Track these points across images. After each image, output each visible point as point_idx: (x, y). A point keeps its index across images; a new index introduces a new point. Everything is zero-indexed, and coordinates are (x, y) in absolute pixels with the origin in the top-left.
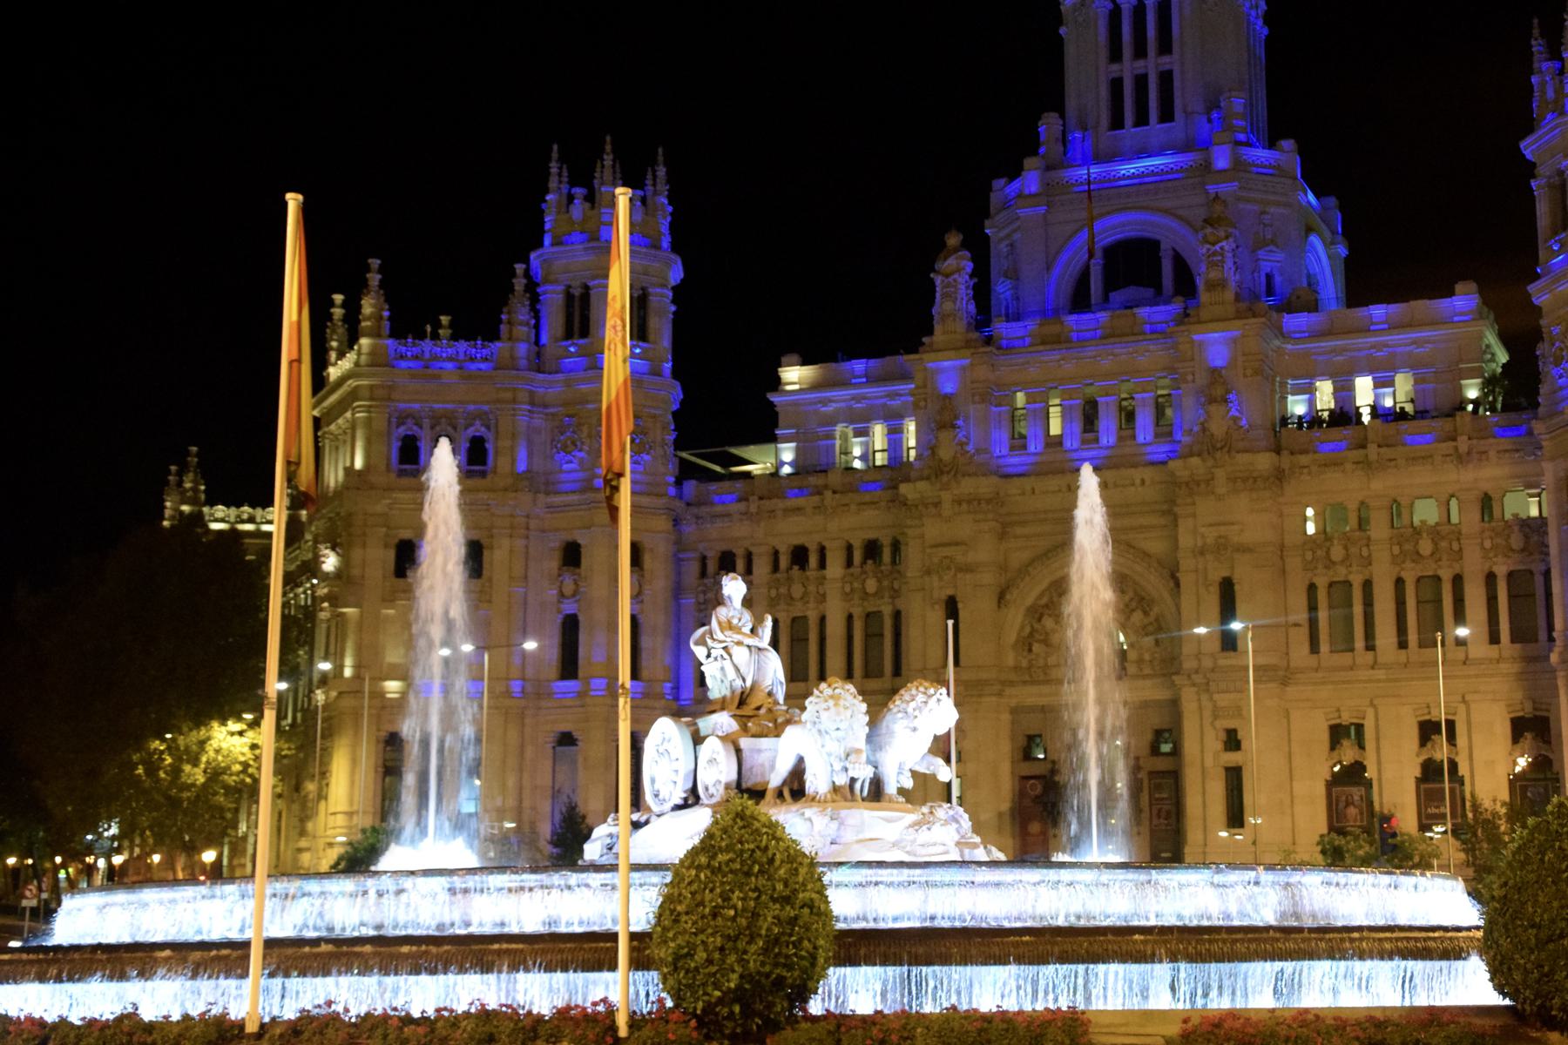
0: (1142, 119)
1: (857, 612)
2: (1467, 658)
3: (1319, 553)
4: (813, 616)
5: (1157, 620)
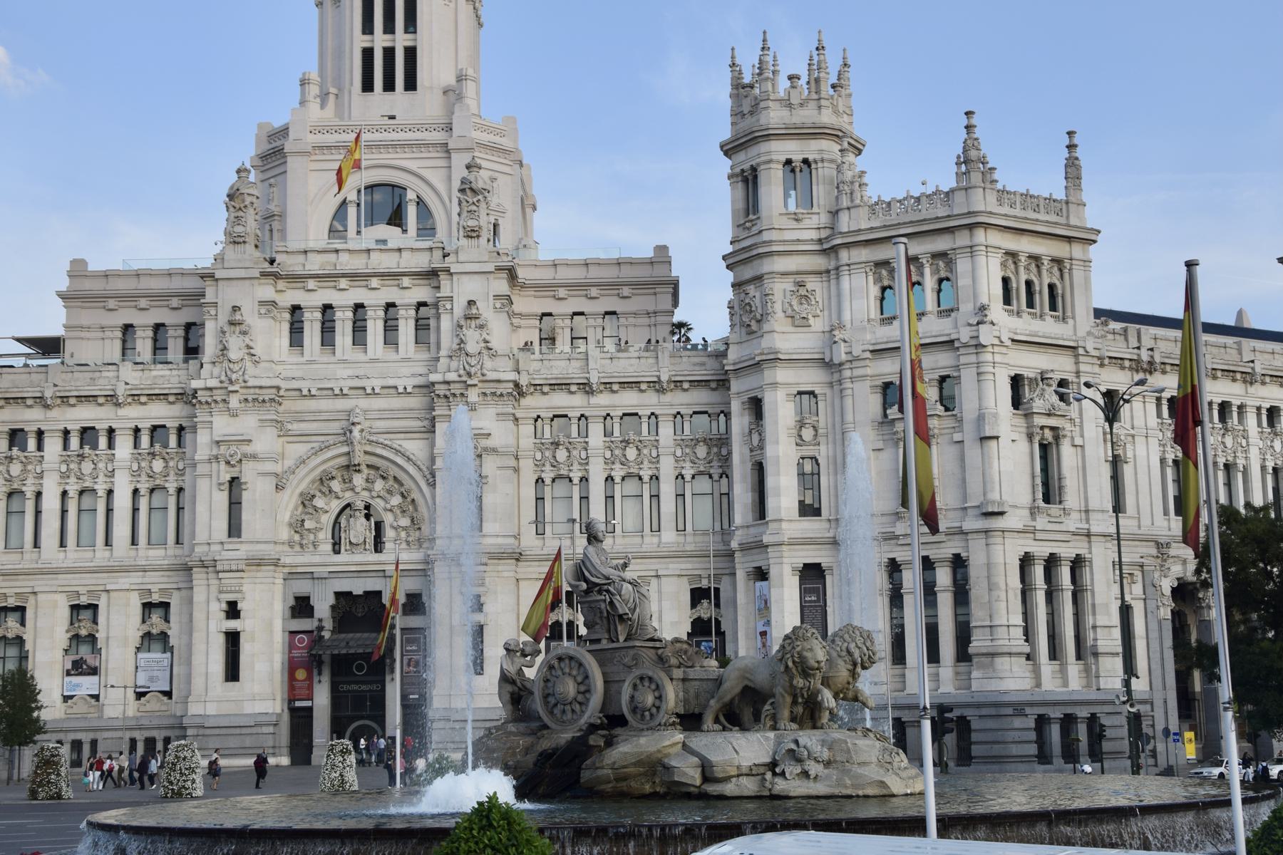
0: (389, 86)
1: (144, 488)
2: (660, 542)
3: (547, 454)
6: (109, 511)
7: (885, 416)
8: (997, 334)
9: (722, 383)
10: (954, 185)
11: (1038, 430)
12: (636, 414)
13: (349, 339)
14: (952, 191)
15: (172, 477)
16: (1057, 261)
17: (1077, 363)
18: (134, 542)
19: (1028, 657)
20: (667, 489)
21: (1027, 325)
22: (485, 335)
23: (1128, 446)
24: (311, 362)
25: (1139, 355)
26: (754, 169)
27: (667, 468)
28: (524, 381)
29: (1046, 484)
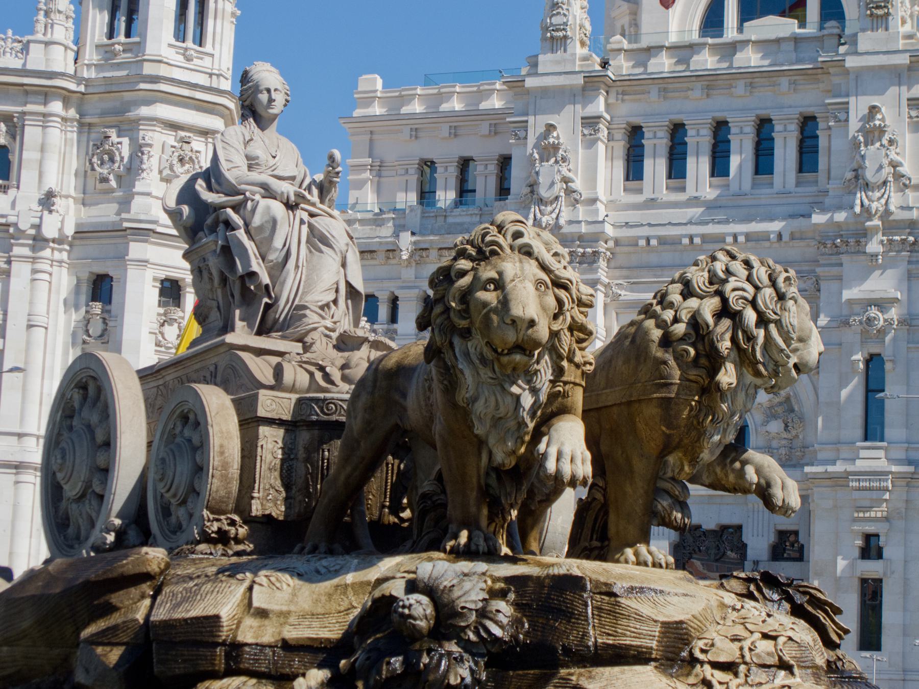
5: (788, 399)
24: (651, 203)
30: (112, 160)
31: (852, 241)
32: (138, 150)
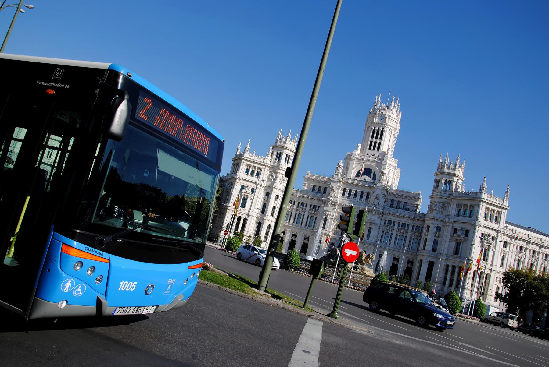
1: (310, 216)
4: (303, 214)
6: (303, 218)
7: (453, 235)
8: (480, 224)
9: (424, 221)
10: (479, 191)
11: (485, 245)
12: (405, 223)
13: (353, 197)
14: (478, 192)
15: (315, 215)
16: (498, 212)
17: (497, 234)
18: (306, 225)
19: (471, 291)
20: (408, 240)
21: (488, 223)
22: (379, 201)
23: (507, 254)
24: (345, 200)
25: (514, 235)
26: (439, 180)
27: (409, 235)
28: (385, 212)
29: (484, 257)
30: (273, 177)
31: (371, 211)
32: (277, 176)
